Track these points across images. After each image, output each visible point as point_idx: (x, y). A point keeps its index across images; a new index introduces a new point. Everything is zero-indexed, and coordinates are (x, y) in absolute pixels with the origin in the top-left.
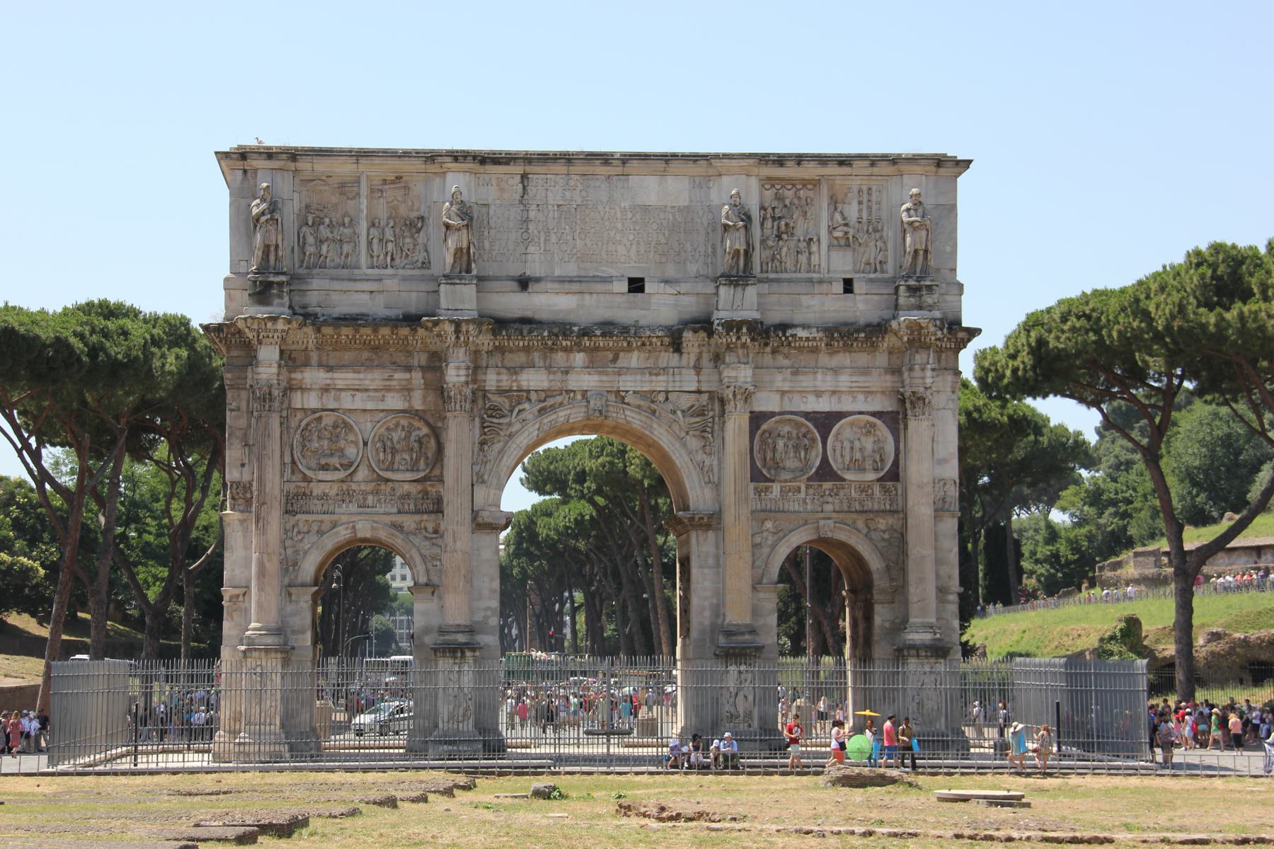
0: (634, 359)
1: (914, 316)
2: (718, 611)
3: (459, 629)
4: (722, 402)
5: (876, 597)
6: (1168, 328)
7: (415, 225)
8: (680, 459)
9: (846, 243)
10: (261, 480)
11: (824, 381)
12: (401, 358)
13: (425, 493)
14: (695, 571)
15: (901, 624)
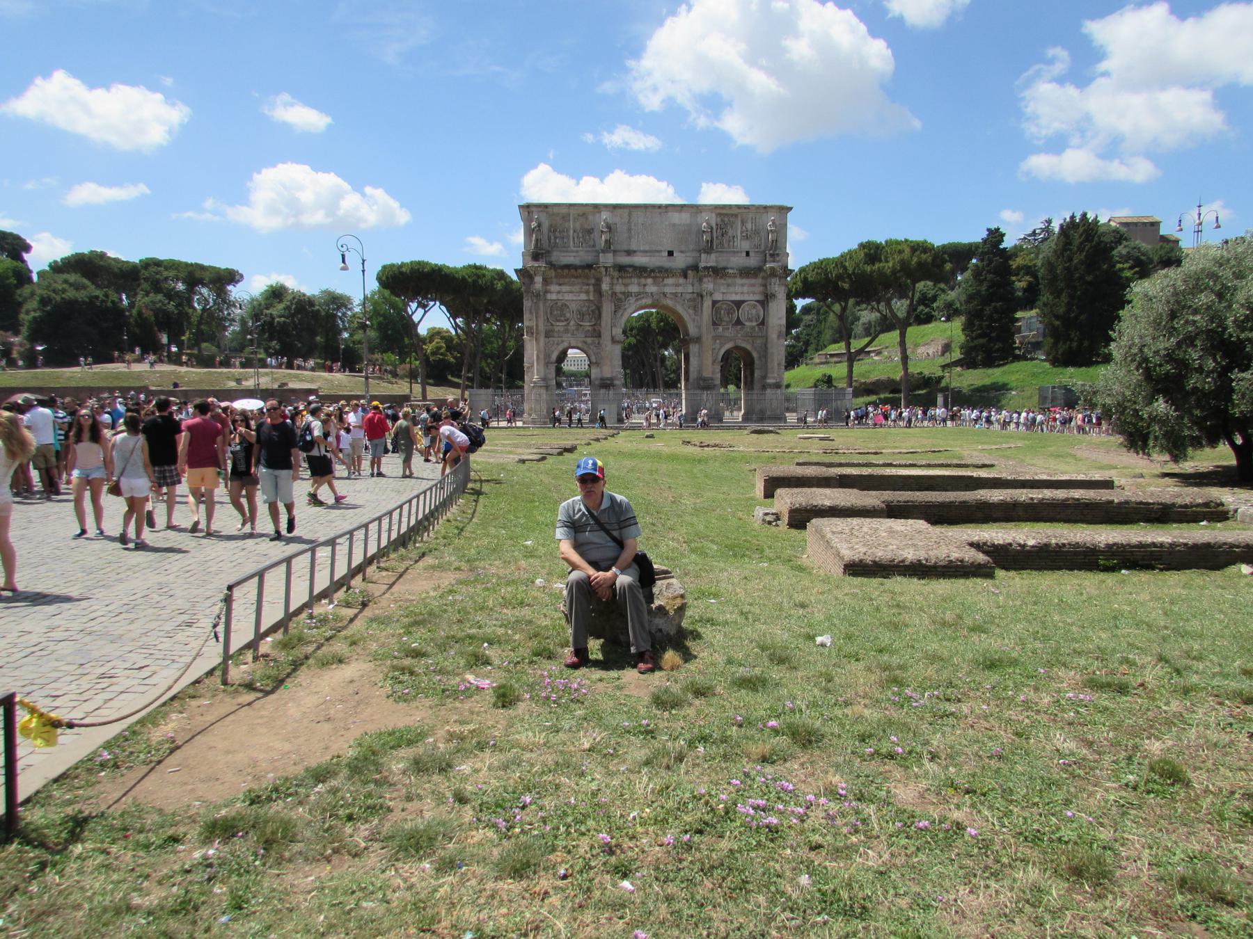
0: (670, 281)
1: (772, 265)
2: (699, 372)
3: (607, 379)
4: (702, 297)
5: (756, 366)
6: (854, 273)
7: (590, 231)
8: (686, 317)
9: (747, 238)
10: (537, 325)
11: (738, 289)
12: (585, 281)
13: (594, 330)
14: (691, 359)
15: (765, 377)
